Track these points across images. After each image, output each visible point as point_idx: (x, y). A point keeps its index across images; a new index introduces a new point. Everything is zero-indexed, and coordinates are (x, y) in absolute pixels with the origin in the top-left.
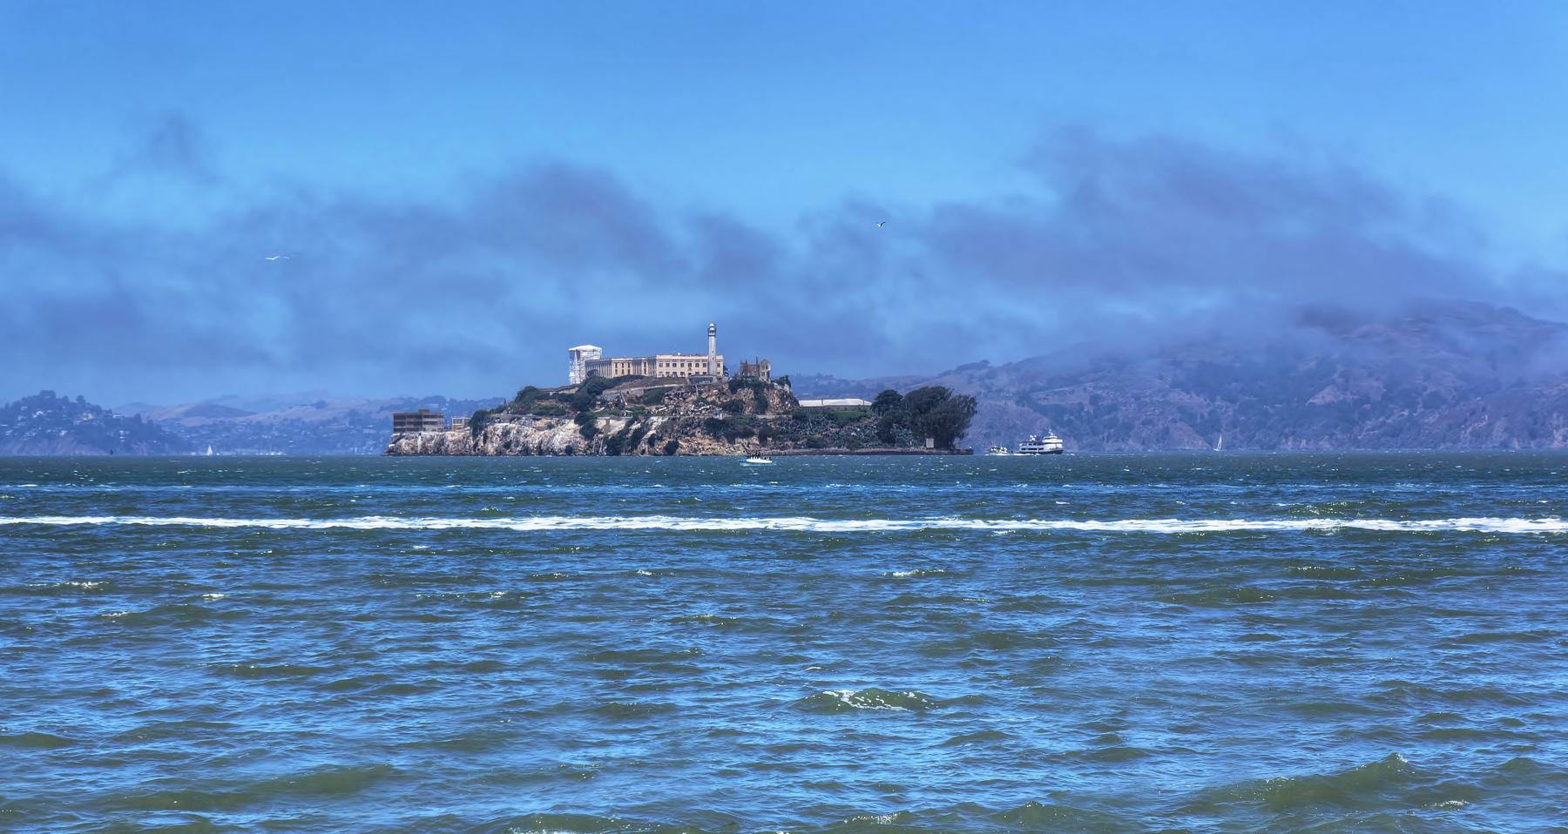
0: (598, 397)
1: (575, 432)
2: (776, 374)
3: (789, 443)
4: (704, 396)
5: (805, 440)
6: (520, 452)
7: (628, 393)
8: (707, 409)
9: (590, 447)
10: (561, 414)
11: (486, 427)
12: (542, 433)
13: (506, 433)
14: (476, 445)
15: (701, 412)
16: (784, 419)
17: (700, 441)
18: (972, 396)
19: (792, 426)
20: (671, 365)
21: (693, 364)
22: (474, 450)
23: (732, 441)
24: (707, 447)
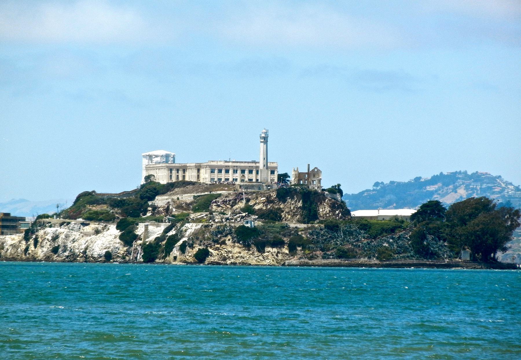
0: (150, 203)
1: (115, 238)
2: (326, 184)
3: (318, 253)
4: (251, 203)
5: (335, 250)
6: (67, 257)
7: (178, 199)
8: (243, 217)
9: (128, 253)
10: (108, 219)
11: (37, 231)
12: (88, 238)
13: (55, 238)
14: (27, 249)
15: (236, 220)
16: (316, 228)
17: (230, 250)
18: (516, 208)
19: (323, 235)
20: (223, 171)
21: (247, 172)
22: (25, 255)
23: (261, 249)
24: (237, 255)
